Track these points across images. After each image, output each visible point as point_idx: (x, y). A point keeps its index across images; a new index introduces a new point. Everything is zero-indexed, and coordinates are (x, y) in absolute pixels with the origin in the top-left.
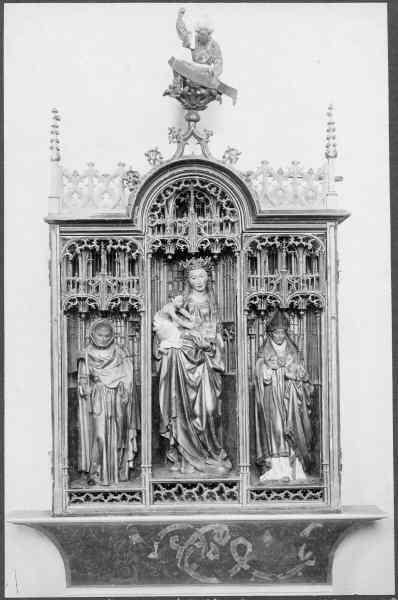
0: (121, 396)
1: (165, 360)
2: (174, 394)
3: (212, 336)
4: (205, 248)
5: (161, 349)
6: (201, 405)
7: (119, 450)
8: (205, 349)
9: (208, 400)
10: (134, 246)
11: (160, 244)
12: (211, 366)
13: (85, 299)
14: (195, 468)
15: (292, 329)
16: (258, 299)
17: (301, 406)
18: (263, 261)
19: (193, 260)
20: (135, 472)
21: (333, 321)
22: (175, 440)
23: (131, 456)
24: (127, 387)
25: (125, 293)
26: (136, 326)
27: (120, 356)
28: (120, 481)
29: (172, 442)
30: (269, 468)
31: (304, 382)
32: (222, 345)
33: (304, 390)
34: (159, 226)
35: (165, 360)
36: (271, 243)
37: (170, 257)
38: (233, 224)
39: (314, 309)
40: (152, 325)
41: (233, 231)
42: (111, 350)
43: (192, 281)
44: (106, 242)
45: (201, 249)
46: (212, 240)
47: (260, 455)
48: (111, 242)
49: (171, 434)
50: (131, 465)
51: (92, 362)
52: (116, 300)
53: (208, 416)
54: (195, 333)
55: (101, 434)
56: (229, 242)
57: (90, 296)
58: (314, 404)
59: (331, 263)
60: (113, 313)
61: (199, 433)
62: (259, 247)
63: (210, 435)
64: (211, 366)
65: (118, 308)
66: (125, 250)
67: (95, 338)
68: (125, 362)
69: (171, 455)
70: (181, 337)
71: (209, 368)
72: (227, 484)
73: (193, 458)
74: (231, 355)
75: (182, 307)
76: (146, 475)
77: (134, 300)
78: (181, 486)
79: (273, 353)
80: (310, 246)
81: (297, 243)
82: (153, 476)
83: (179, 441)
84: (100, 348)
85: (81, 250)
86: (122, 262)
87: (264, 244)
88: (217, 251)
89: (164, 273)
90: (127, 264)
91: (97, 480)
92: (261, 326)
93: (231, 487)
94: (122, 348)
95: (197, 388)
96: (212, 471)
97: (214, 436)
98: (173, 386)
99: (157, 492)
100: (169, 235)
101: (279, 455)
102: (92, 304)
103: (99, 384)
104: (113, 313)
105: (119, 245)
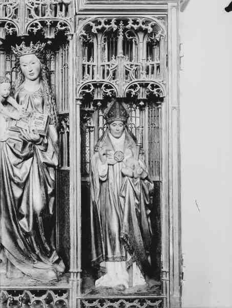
4: (35, 30)
6: (28, 204)
8: (34, 142)
9: (36, 197)
15: (134, 122)
16: (92, 88)
17: (139, 206)
18: (99, 44)
21: (175, 112)
30: (104, 273)
31: (141, 179)
33: (143, 189)
36: (107, 26)
39: (154, 100)
45: (31, 33)
47: (95, 259)
53: (35, 215)
54: (21, 124)
56: (62, 25)
58: (153, 201)
59: (173, 47)
61: (27, 235)
62: (94, 30)
63: (38, 237)
64: (43, 160)
72: (56, 291)
73: (20, 262)
74: (61, 149)
79: (110, 147)
80: (150, 30)
81: (136, 27)
88: (50, 35)
92: (101, 118)
93: (60, 295)
95: (23, 185)
97: (44, 239)
101: (114, 259)
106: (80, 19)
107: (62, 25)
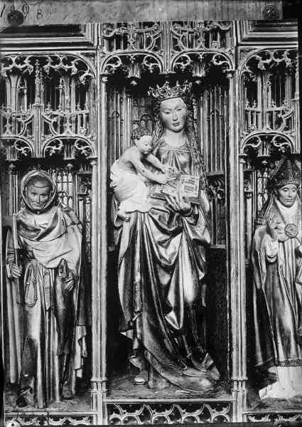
0: (63, 280)
1: (127, 227)
2: (138, 278)
3: (194, 194)
4: (183, 66)
5: (121, 213)
7: (61, 357)
8: (183, 213)
10: (82, 66)
11: (120, 63)
12: (192, 237)
13: (12, 142)
14: (168, 381)
19: (166, 87)
20: (83, 388)
22: (141, 342)
23: (78, 362)
24: (72, 266)
25: (69, 133)
26: (86, 179)
27: (64, 223)
28: (62, 399)
29: (136, 345)
30: (273, 381)
32: (207, 209)
34: (117, 37)
35: (127, 227)
36: (278, 60)
37: (134, 83)
38: (223, 33)
40: (109, 181)
41: (224, 45)
42: (51, 214)
43: (165, 116)
44: (43, 61)
45: (177, 69)
46: (194, 57)
48: (50, 60)
49: (135, 334)
50: (80, 374)
51: (22, 232)
52: (56, 143)
54: (168, 190)
55: (35, 333)
56: (218, 59)
57: (20, 137)
60: (53, 162)
64: (192, 237)
65: (58, 155)
66: (70, 70)
67: (29, 198)
68: (69, 229)
69: (134, 360)
70: (149, 196)
71: (188, 239)
72: (214, 405)
73: (165, 368)
75: (151, 152)
76: (98, 392)
77: (82, 143)
78: (148, 407)
82: (108, 394)
83: (146, 344)
84: (35, 212)
85: (8, 72)
86: (67, 91)
87: (268, 61)
89: (127, 110)
90: (73, 95)
91: (30, 399)
93: (219, 409)
94: (67, 212)
96: (193, 386)
98: (137, 265)
99: (114, 415)
100: (132, 50)
102: (22, 149)
103: (34, 262)
104: (53, 162)
105: (61, 65)
106: (242, 51)
107: (218, 59)
